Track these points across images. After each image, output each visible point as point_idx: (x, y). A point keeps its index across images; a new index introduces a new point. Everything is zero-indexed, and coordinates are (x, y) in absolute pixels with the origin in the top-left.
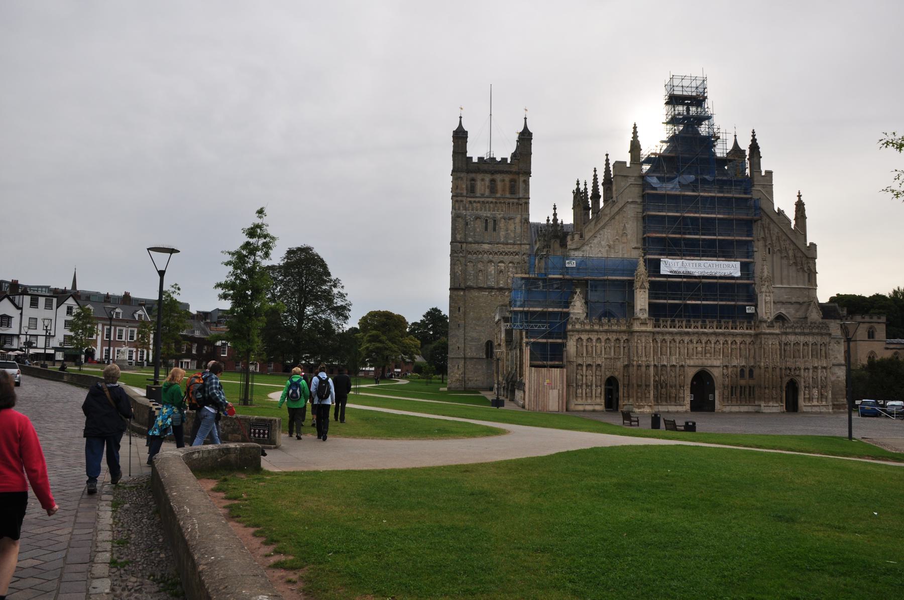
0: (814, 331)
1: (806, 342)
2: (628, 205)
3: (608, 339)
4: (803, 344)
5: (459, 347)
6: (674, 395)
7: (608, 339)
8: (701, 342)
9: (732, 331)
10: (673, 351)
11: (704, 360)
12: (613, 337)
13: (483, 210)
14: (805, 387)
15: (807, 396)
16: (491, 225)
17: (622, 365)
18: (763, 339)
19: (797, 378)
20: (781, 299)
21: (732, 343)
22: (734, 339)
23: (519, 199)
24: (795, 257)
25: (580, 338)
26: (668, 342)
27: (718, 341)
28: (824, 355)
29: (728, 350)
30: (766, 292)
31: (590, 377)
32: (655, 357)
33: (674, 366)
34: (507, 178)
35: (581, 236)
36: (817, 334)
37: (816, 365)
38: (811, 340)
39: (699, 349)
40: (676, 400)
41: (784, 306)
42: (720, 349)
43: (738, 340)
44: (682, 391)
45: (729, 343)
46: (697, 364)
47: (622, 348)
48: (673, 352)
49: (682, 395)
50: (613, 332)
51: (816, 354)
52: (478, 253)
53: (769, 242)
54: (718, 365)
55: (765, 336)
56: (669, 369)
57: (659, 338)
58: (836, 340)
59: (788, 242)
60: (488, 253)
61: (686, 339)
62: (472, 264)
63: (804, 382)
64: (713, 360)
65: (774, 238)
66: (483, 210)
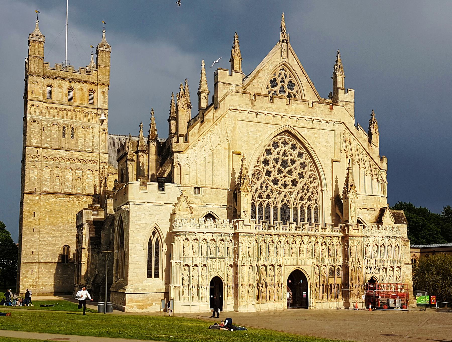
5: (33, 252)
12: (217, 238)
13: (60, 118)
16: (68, 132)
18: (349, 240)
22: (324, 241)
23: (97, 109)
26: (268, 243)
27: (310, 242)
28: (397, 254)
34: (86, 87)
35: (186, 140)
39: (295, 250)
45: (320, 244)
52: (55, 159)
53: (349, 154)
54: (311, 265)
55: (352, 238)
59: (365, 155)
60: (66, 160)
62: (49, 170)
65: (354, 151)
66: (60, 118)
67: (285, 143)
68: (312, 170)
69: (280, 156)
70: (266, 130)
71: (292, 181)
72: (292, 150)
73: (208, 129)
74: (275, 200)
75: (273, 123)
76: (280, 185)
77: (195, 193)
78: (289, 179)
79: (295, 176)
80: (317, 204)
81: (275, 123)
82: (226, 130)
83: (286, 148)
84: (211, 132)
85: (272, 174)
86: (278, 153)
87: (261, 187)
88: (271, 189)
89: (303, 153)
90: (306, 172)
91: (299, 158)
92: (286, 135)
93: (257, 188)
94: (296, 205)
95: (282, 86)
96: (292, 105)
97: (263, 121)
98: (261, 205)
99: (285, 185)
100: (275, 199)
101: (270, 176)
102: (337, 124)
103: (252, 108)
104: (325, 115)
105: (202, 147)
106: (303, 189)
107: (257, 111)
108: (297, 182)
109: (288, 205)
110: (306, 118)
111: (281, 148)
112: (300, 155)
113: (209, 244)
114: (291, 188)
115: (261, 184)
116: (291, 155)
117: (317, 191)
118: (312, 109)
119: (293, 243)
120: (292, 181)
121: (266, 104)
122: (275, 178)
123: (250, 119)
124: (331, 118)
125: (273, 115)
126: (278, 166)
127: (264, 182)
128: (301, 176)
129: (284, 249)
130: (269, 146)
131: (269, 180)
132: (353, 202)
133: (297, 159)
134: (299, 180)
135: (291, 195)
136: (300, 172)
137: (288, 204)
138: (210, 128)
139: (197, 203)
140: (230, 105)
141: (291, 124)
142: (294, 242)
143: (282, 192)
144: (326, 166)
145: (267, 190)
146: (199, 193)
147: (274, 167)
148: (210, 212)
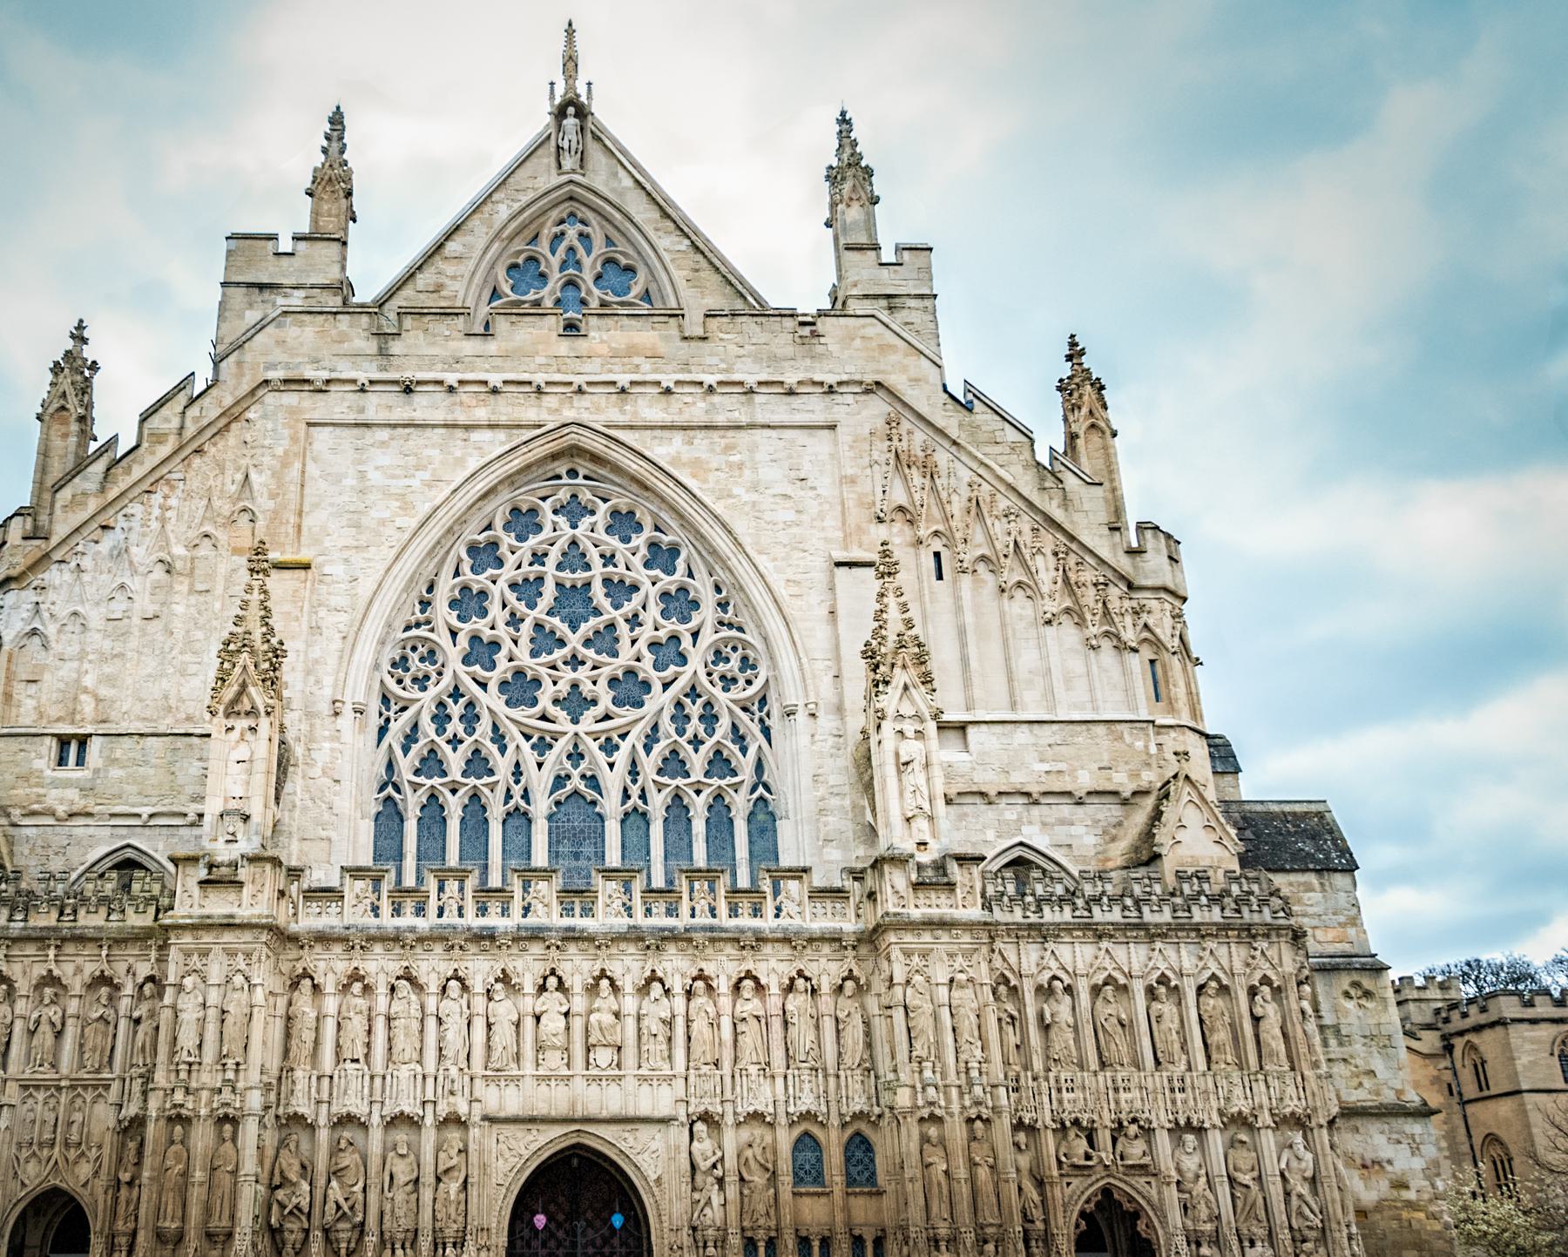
2: (271, 399)
3: (51, 980)
7: (51, 980)
8: (561, 986)
9: (733, 922)
10: (400, 1043)
11: (579, 1083)
12: (79, 970)
17: (112, 1123)
21: (737, 987)
22: (749, 965)
27: (653, 978)
32: (299, 1074)
33: (400, 1120)
39: (553, 1023)
42: (669, 1023)
43: (773, 967)
45: (723, 986)
46: (542, 1109)
47: (123, 1024)
48: (405, 1044)
56: (376, 1135)
61: (480, 969)
64: (630, 1083)
67: (574, 510)
68: (730, 626)
69: (550, 568)
70: (458, 454)
71: (613, 682)
72: (614, 542)
73: (157, 475)
74: (517, 782)
75: (494, 419)
77: (62, 761)
78: (595, 672)
80: (767, 788)
81: (503, 419)
82: (243, 470)
83: (577, 532)
84: (173, 488)
85: (501, 658)
86: (538, 558)
87: (441, 719)
88: (495, 727)
89: (674, 551)
90: (695, 635)
91: (657, 572)
92: (582, 472)
93: (415, 727)
94: (643, 796)
96: (592, 334)
97: (439, 416)
99: (576, 703)
100: (517, 772)
101: (492, 666)
103: (383, 369)
104: (774, 359)
105: (120, 553)
106: (680, 717)
107: (408, 375)
108: (646, 686)
109: (594, 803)
110: (672, 385)
111: (555, 530)
112: (661, 556)
113: (21, 1006)
114: (607, 717)
117: (761, 720)
118: (701, 344)
119: (542, 988)
120: (613, 682)
121: (453, 344)
122: (519, 673)
123: (371, 415)
124: (806, 370)
125: (491, 385)
126: (539, 612)
127: (456, 694)
128: (668, 651)
129: (489, 1026)
130: (489, 527)
131: (483, 686)
132: (910, 733)
133: (641, 575)
134: (655, 678)
135: (609, 747)
136: (663, 635)
137: (591, 794)
138: (165, 471)
139: (61, 810)
140: (272, 366)
141: (595, 417)
142: (552, 982)
144: (795, 590)
145: (470, 731)
146: (80, 761)
147: (515, 621)
148: (129, 854)
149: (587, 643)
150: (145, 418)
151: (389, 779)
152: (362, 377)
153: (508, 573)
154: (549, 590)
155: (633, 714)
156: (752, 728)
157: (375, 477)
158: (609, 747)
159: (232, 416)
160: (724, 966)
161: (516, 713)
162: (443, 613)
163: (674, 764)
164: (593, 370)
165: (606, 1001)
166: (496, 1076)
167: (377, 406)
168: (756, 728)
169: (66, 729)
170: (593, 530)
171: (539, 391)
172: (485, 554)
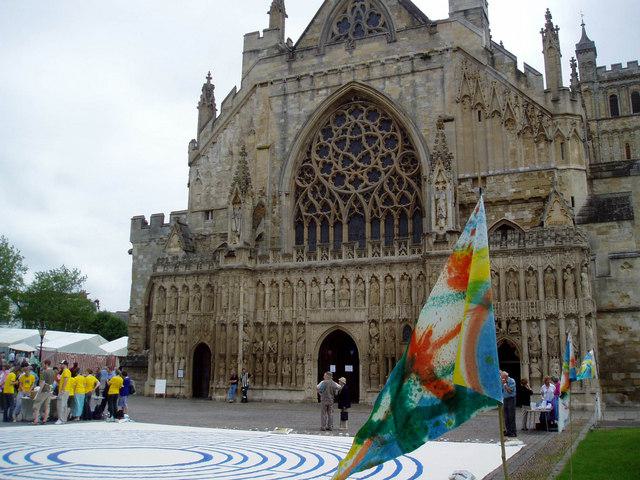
0: (547, 244)
1: (531, 269)
4: (527, 273)
6: (286, 373)
8: (332, 282)
14: (531, 357)
15: (536, 374)
19: (515, 338)
20: (503, 195)
24: (528, 117)
25: (162, 287)
26: (281, 285)
27: (358, 278)
29: (378, 291)
30: (438, 183)
31: (172, 345)
33: (286, 324)
36: (553, 250)
37: (553, 312)
38: (540, 263)
39: (329, 293)
40: (293, 381)
41: (510, 207)
43: (397, 273)
44: (299, 367)
45: (381, 279)
46: (327, 319)
49: (299, 374)
50: (203, 274)
51: (557, 290)
57: (266, 279)
58: (622, 261)
61: (308, 277)
63: (530, 347)
64: (352, 311)
67: (356, 112)
69: (348, 136)
71: (368, 173)
72: (368, 122)
76: (347, 184)
79: (375, 162)
86: (344, 131)
87: (314, 192)
88: (331, 194)
89: (390, 122)
90: (396, 153)
91: (384, 132)
95: (358, 25)
98: (312, 224)
99: (356, 182)
102: (448, 55)
106: (391, 183)
108: (379, 173)
112: (386, 123)
114: (366, 186)
115: (314, 188)
116: (367, 128)
122: (338, 174)
128: (387, 160)
131: (327, 179)
133: (378, 133)
134: (381, 169)
143: (350, 195)
147: (337, 155)
149: (360, 161)
150: (222, 104)
151: (299, 214)
152: (285, 78)
153: (334, 139)
154: (348, 140)
155: (375, 184)
156: (414, 185)
157: (289, 112)
158: (367, 196)
159: (247, 99)
160: (381, 274)
161: (336, 188)
162: (314, 156)
163: (388, 201)
164: (358, 61)
165: (346, 286)
166: (314, 310)
167: (291, 86)
168: (414, 185)
169: (207, 208)
170: (362, 119)
171: (341, 72)
172: (327, 132)
